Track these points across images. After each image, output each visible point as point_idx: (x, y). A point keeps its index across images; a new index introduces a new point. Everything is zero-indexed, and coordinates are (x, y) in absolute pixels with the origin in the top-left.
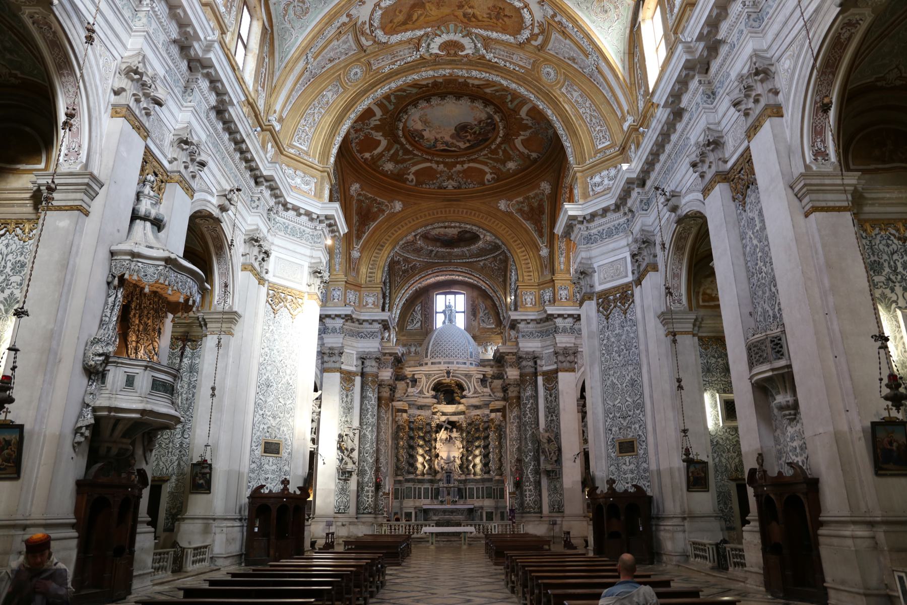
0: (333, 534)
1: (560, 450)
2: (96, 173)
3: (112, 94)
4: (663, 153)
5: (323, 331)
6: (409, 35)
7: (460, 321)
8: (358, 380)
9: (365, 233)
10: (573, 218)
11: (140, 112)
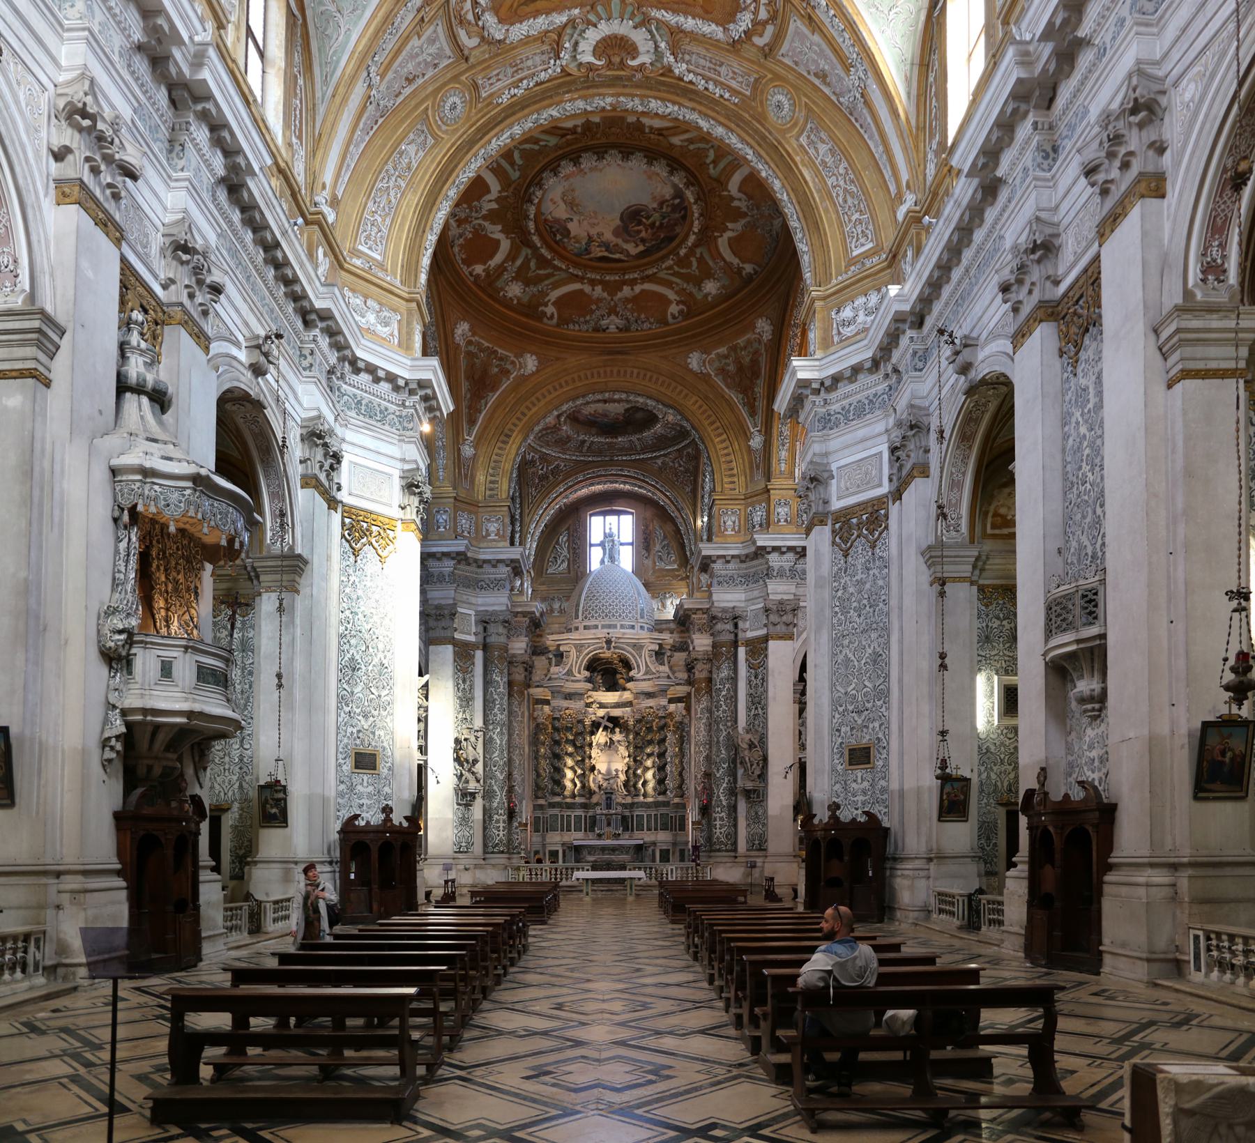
0: (453, 881)
1: (765, 759)
2: (49, 309)
3: (51, 160)
4: (957, 265)
5: (427, 578)
6: (541, 23)
7: (626, 559)
8: (479, 655)
10: (804, 384)
11: (103, 192)
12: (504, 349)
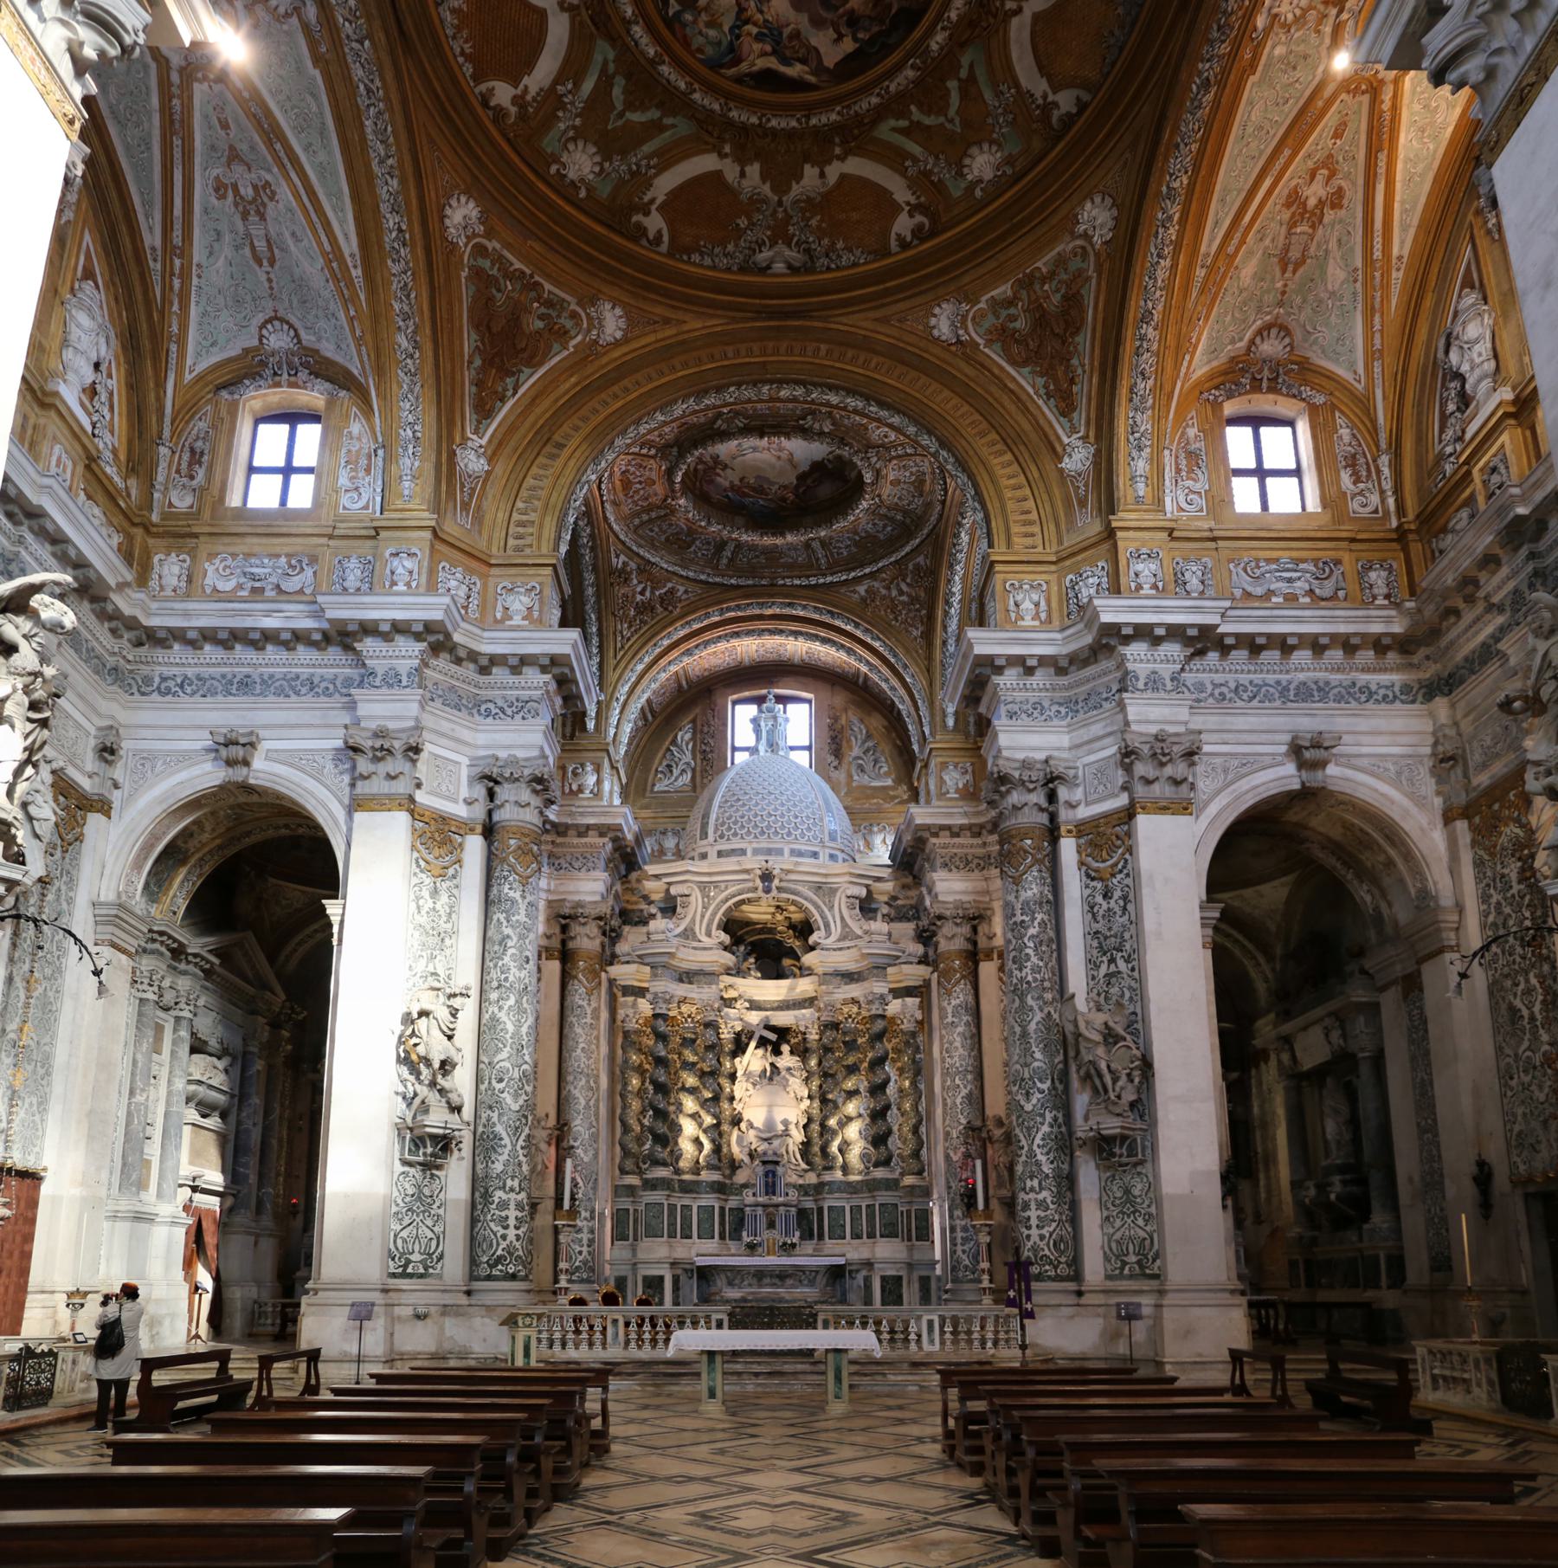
1: (1147, 1065)
8: (474, 846)
9: (503, 400)
12: (557, 283)
